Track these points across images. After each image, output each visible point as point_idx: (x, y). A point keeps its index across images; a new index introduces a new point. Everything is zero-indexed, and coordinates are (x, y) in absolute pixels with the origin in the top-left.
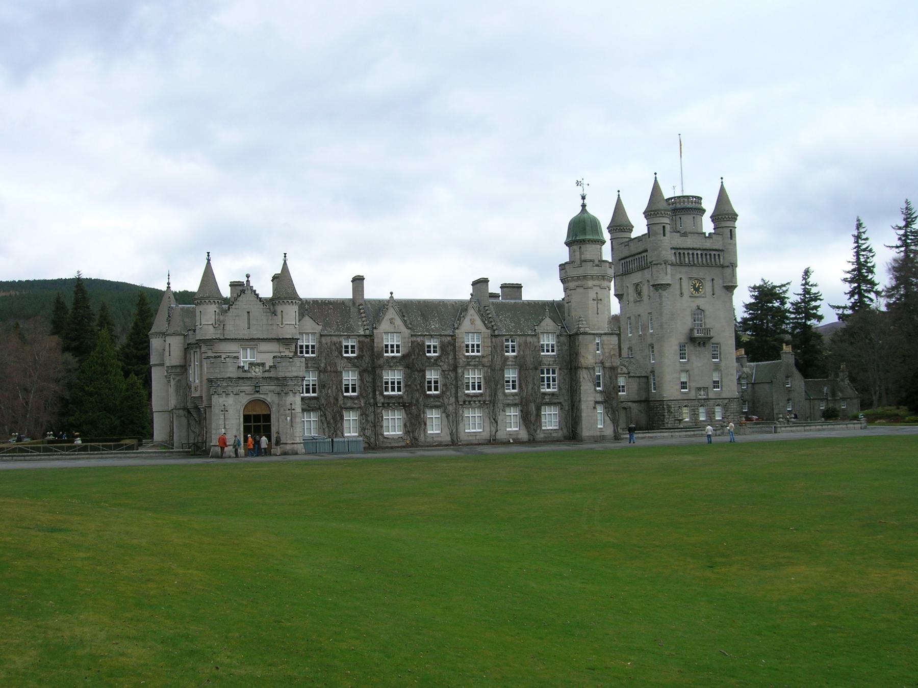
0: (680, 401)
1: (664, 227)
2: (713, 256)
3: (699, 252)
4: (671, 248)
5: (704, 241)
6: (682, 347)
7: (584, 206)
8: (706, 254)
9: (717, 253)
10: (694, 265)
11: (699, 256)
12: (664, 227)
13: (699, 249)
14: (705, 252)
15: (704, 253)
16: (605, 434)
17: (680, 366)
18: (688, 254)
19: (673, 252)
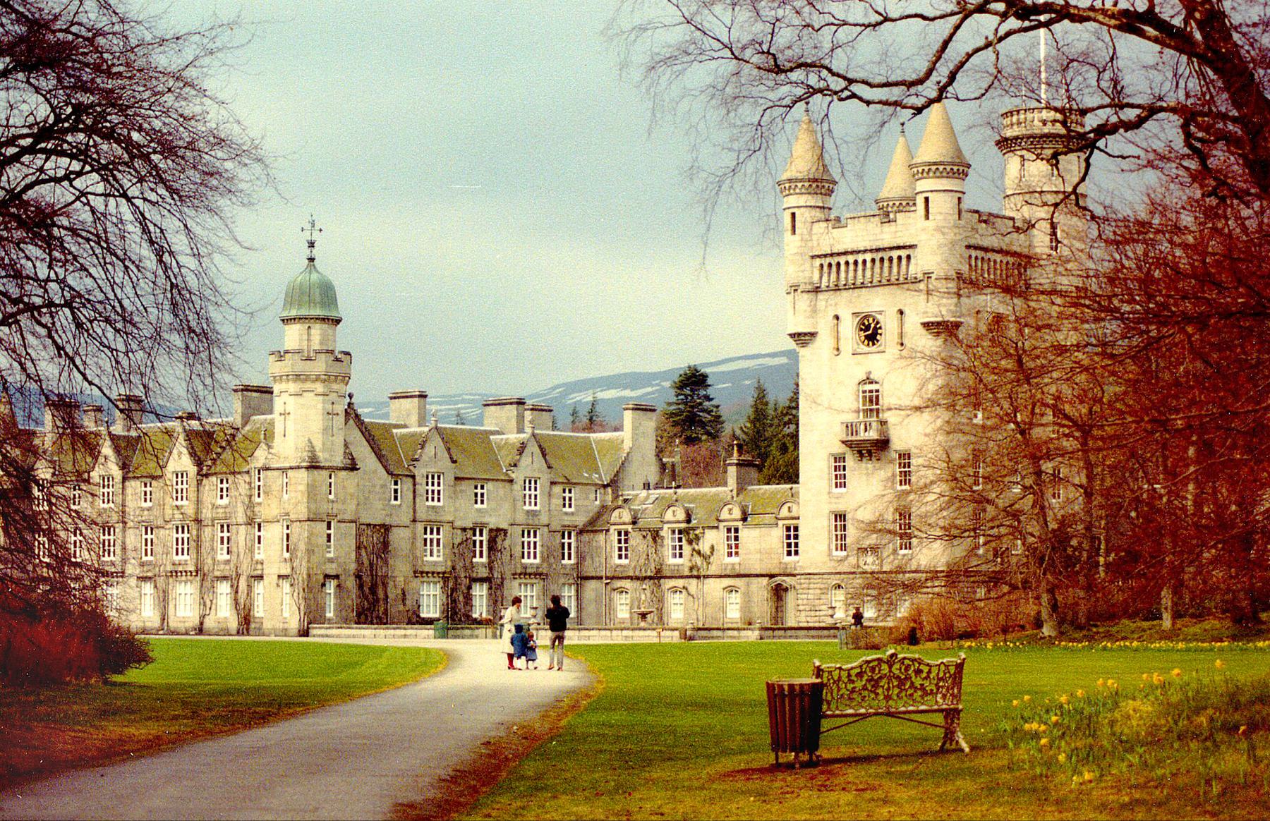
0: (825, 576)
1: (793, 215)
2: (895, 261)
3: (868, 257)
4: (813, 257)
5: (878, 230)
6: (839, 459)
7: (311, 260)
8: (882, 260)
9: (903, 253)
10: (863, 286)
11: (869, 264)
12: (793, 215)
13: (865, 251)
14: (880, 255)
15: (878, 256)
16: (286, 626)
17: (830, 503)
18: (847, 263)
19: (818, 262)
